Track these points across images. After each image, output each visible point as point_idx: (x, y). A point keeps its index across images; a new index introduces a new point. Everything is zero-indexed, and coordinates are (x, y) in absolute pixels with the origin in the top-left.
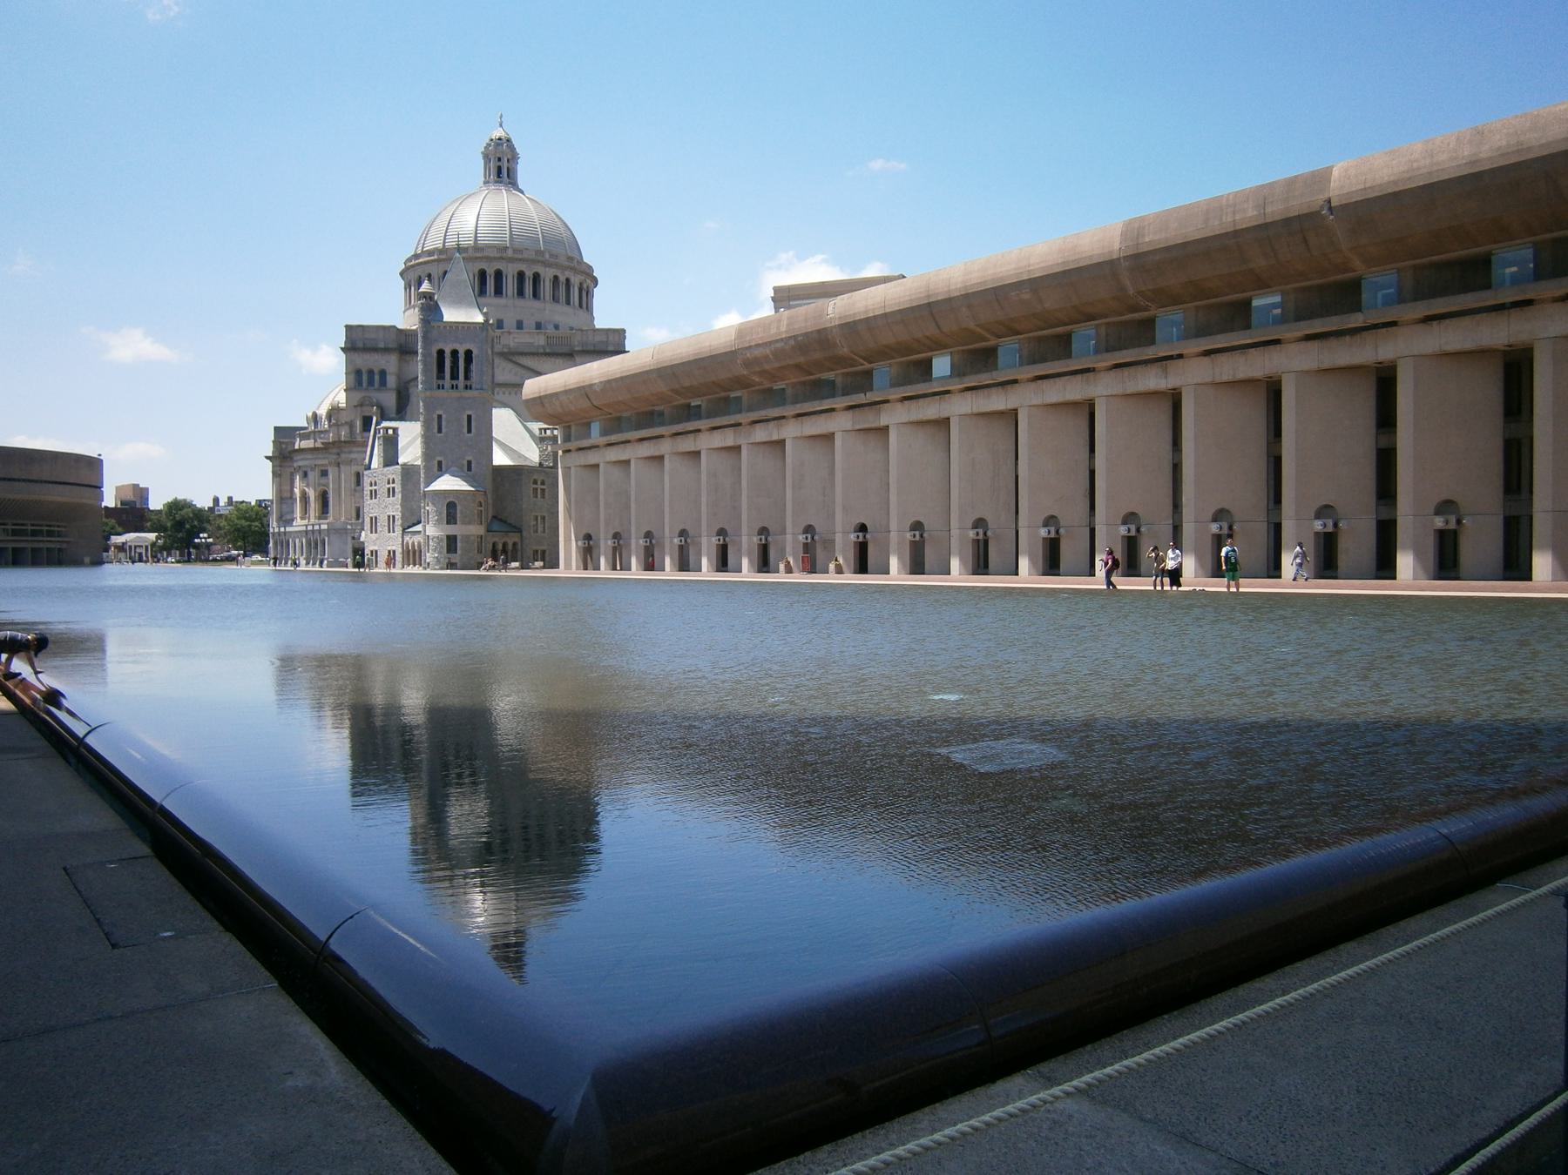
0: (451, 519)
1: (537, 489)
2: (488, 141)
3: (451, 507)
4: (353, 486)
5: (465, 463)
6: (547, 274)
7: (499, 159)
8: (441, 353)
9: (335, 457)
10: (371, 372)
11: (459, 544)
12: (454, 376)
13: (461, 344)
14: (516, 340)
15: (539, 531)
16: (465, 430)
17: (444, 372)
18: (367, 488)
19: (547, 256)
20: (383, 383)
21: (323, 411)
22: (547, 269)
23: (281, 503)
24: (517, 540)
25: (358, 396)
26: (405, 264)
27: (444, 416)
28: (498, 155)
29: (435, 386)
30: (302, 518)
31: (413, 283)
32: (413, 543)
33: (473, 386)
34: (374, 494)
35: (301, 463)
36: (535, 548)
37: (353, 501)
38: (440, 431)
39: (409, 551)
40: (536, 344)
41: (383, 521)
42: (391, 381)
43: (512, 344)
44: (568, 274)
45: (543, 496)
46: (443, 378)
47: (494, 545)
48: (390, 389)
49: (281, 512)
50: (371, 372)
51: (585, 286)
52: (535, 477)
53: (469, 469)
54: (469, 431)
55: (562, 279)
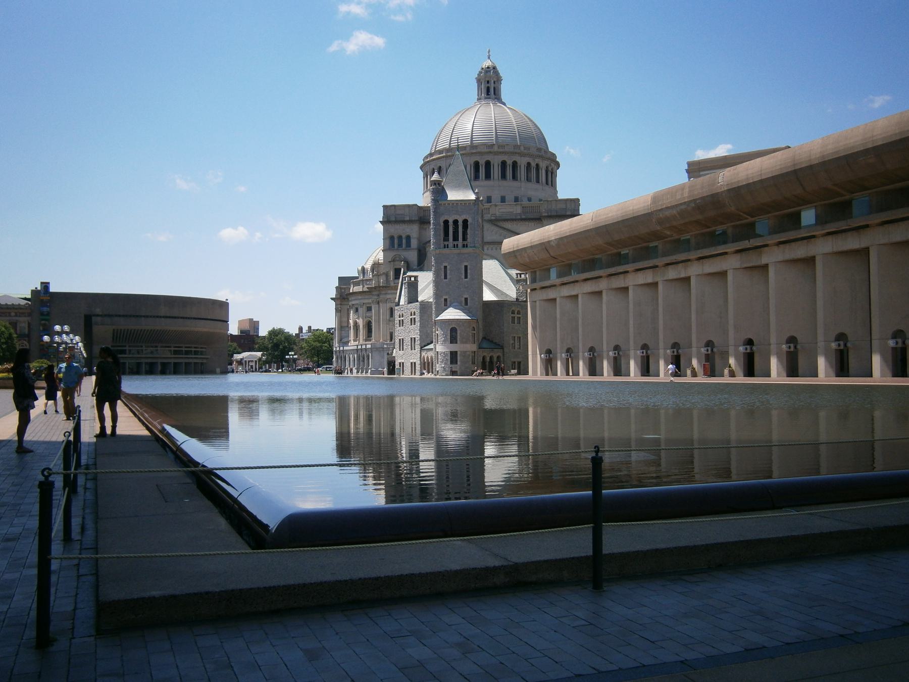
0: (453, 340)
1: (514, 317)
2: (480, 70)
3: (453, 331)
6: (522, 162)
7: (488, 82)
8: (446, 223)
9: (376, 297)
10: (400, 237)
12: (456, 238)
13: (460, 215)
14: (501, 210)
15: (516, 348)
16: (463, 277)
18: (397, 319)
19: (522, 148)
20: (408, 244)
21: (368, 266)
22: (522, 158)
23: (341, 330)
24: (501, 354)
25: (392, 254)
26: (423, 160)
27: (448, 267)
28: (487, 79)
29: (442, 246)
30: (354, 341)
31: (429, 173)
32: (428, 357)
33: (469, 246)
34: (401, 323)
35: (354, 302)
36: (513, 360)
38: (446, 277)
39: (425, 363)
40: (515, 213)
41: (407, 342)
42: (414, 243)
44: (537, 160)
45: (519, 323)
47: (484, 358)
49: (341, 336)
51: (550, 169)
52: (513, 308)
53: (466, 303)
54: (466, 277)
55: (533, 165)
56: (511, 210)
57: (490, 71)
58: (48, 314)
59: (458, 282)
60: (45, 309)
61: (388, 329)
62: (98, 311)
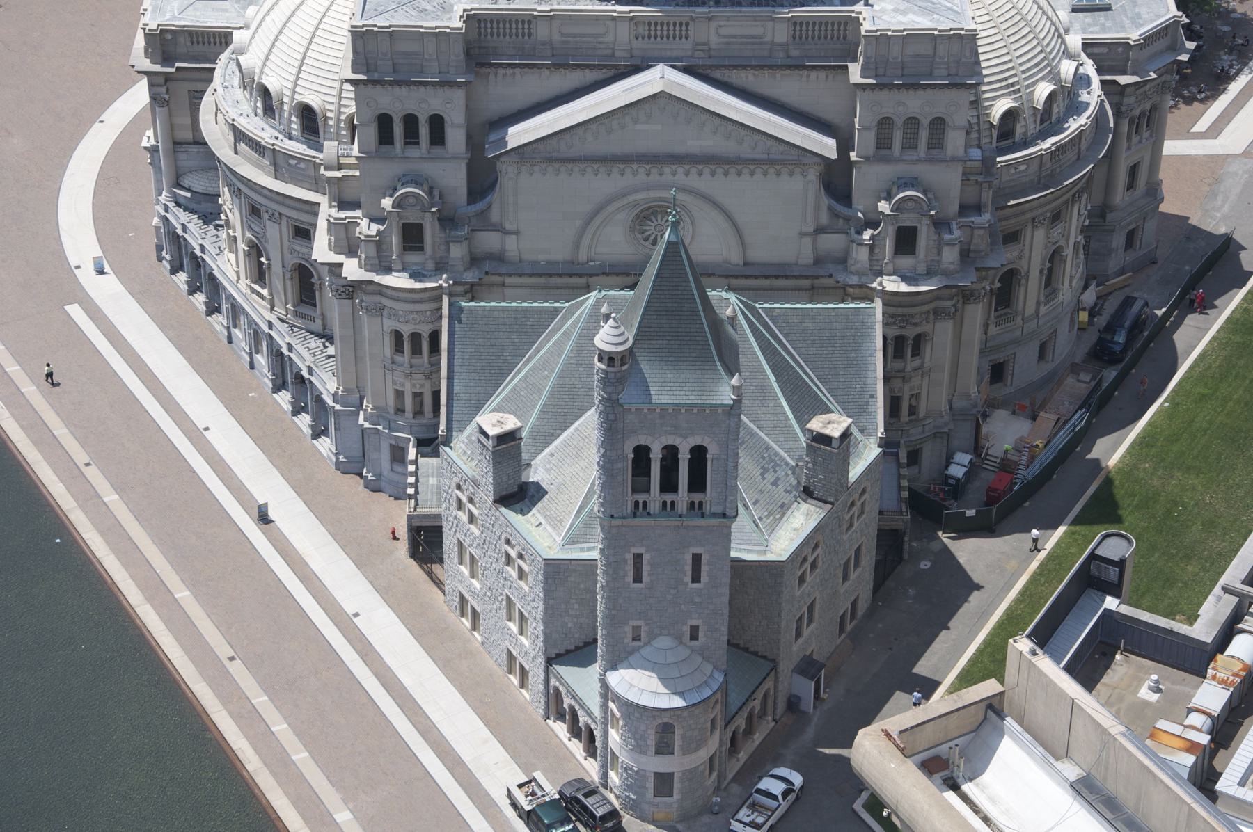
3: (666, 730)
5: (687, 629)
8: (642, 454)
10: (411, 122)
11: (677, 786)
12: (669, 484)
14: (723, 31)
16: (688, 578)
17: (648, 474)
27: (646, 557)
29: (630, 507)
33: (707, 508)
37: (389, 377)
38: (638, 578)
40: (768, 39)
42: (456, 138)
43: (714, 41)
46: (648, 490)
48: (455, 157)
49: (176, 167)
53: (694, 637)
54: (696, 578)
56: (758, 31)
59: (673, 592)
61: (389, 384)
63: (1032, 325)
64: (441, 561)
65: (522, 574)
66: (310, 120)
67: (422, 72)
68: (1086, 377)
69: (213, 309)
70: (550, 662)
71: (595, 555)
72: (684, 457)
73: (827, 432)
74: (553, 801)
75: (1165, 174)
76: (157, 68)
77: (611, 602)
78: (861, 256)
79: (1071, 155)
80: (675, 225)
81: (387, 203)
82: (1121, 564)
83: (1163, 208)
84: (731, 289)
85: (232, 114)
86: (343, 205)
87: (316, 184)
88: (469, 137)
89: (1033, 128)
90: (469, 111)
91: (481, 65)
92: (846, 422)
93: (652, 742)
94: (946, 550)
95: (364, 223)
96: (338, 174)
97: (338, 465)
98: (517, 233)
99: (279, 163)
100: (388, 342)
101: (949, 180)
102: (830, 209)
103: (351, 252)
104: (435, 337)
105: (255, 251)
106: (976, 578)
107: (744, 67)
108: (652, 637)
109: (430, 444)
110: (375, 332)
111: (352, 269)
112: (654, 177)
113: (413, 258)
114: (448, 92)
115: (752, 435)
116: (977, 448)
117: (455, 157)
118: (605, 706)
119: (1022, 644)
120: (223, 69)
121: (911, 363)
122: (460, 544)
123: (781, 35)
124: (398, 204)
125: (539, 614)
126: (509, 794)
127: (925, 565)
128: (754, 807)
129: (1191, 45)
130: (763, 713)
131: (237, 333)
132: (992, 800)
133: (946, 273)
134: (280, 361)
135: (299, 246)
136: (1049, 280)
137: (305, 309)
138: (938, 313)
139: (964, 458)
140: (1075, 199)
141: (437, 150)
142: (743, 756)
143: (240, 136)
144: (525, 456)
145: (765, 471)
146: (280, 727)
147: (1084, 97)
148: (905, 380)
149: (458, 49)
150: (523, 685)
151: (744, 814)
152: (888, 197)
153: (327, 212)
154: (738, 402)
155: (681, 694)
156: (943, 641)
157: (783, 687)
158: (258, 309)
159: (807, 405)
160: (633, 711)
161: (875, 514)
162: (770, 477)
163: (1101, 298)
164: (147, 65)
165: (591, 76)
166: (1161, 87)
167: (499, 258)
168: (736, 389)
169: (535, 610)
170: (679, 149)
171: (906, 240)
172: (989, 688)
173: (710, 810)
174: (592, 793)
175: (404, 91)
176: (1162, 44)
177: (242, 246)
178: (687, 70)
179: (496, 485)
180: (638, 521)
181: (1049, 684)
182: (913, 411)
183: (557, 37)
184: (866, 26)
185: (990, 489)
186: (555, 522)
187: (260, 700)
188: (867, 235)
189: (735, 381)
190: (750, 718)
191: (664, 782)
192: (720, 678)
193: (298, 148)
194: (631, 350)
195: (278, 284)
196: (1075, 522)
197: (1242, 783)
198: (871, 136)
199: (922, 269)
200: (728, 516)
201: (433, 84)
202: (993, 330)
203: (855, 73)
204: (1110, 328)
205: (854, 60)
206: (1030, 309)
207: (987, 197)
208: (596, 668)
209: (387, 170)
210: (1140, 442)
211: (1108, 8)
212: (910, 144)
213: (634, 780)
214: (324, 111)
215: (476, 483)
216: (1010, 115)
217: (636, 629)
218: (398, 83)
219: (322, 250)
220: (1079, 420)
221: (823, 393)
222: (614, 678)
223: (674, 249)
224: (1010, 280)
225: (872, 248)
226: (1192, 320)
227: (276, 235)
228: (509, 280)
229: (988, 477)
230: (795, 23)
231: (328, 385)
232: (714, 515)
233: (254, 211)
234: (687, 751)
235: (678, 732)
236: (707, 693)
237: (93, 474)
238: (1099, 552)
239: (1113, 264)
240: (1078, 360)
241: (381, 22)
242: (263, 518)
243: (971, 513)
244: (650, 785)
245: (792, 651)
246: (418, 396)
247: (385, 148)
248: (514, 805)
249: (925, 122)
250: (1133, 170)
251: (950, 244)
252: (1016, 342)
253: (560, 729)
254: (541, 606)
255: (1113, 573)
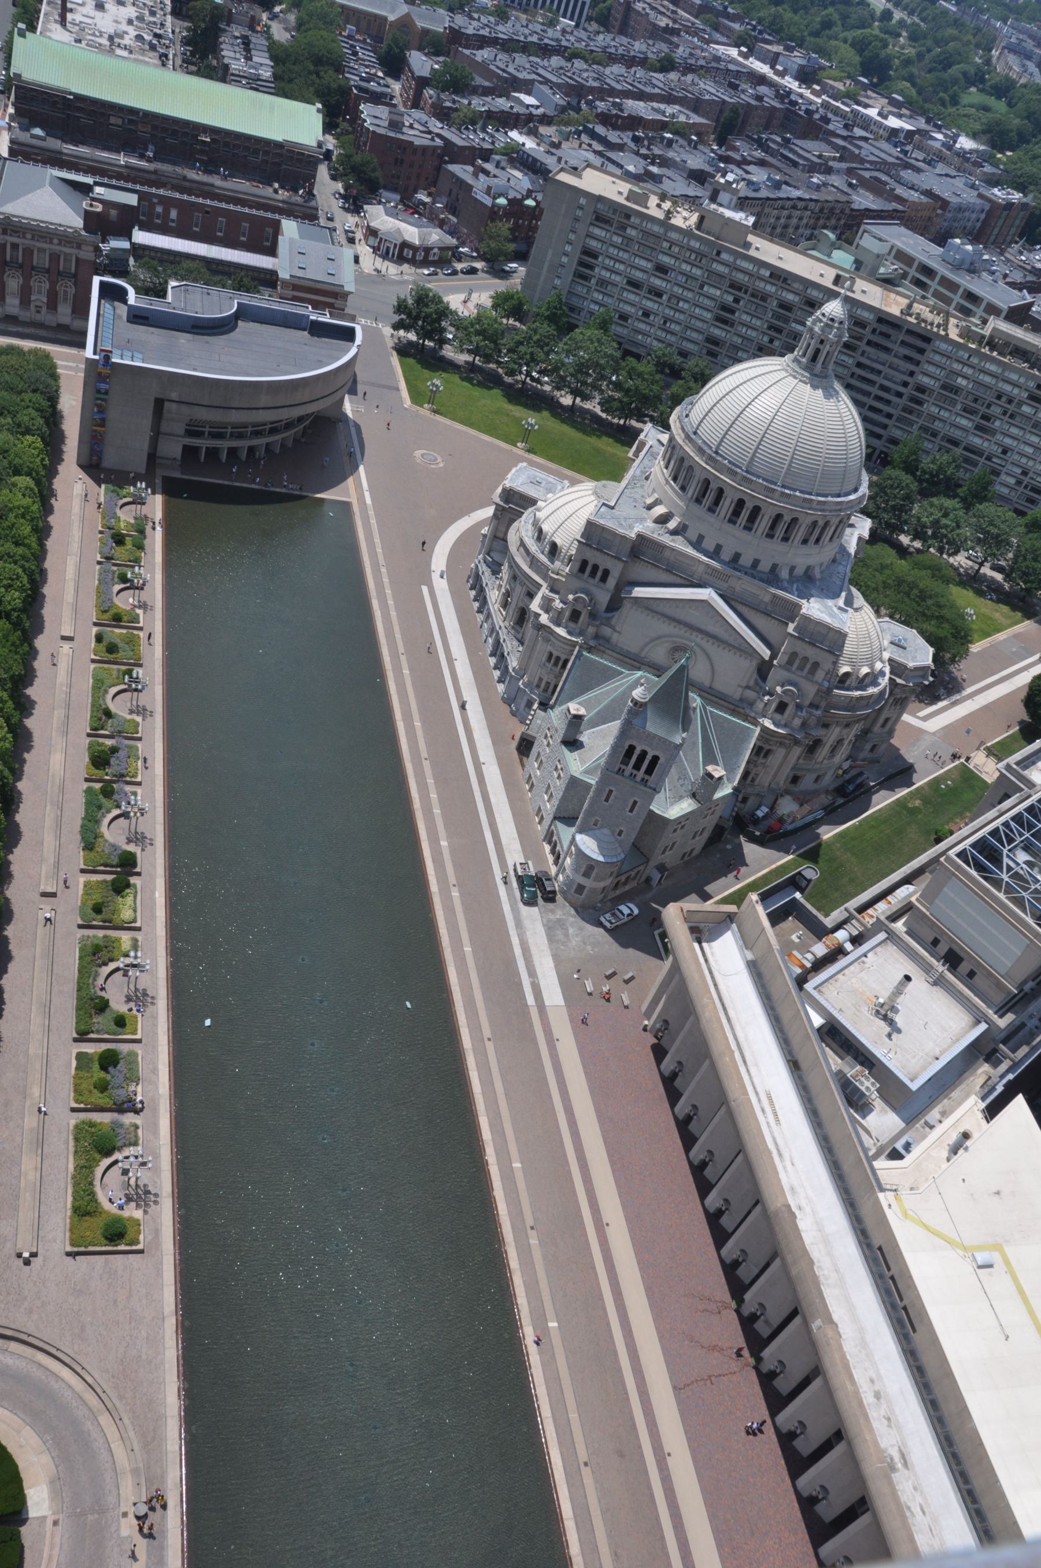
4: (544, 659)
5: (618, 830)
8: (632, 748)
10: (595, 568)
11: (585, 892)
12: (637, 766)
16: (628, 809)
27: (614, 793)
29: (616, 769)
33: (649, 784)
38: (607, 800)
42: (611, 582)
43: (738, 589)
48: (607, 590)
50: (595, 568)
53: (620, 834)
54: (631, 811)
57: (831, 327)
58: (106, 393)
60: (103, 386)
62: (174, 396)
63: (818, 766)
64: (528, 757)
65: (559, 777)
66: (554, 550)
67: (609, 549)
68: (830, 797)
69: (479, 611)
70: (555, 818)
71: (593, 782)
72: (649, 758)
73: (713, 773)
74: (531, 876)
75: (898, 727)
76: (501, 503)
77: (591, 805)
78: (760, 706)
79: (864, 702)
80: (688, 658)
81: (571, 597)
82: (809, 881)
83: (892, 741)
84: (699, 696)
85: (524, 534)
86: (552, 590)
87: (545, 577)
88: (617, 584)
89: (854, 684)
90: (622, 574)
91: (635, 556)
92: (723, 773)
93: (583, 870)
94: (740, 845)
95: (558, 601)
96: (556, 577)
97: (503, 698)
98: (620, 633)
99: (534, 562)
100: (546, 655)
101: (811, 690)
102: (756, 680)
103: (547, 611)
104: (566, 662)
105: (508, 594)
106: (748, 862)
107: (745, 605)
108: (602, 827)
109: (544, 706)
110: (542, 649)
111: (544, 619)
112: (688, 634)
113: (572, 625)
114: (616, 562)
115: (682, 761)
116: (772, 808)
117: (607, 590)
118: (569, 848)
119: (754, 897)
120: (528, 515)
121: (761, 760)
122: (539, 754)
123: (767, 599)
124: (575, 600)
125: (559, 796)
126: (515, 865)
127: (729, 847)
128: (614, 915)
129: (931, 679)
130: (634, 878)
131: (485, 625)
132: (712, 954)
133: (792, 729)
134: (497, 644)
135: (526, 599)
136: (833, 750)
137: (517, 627)
138: (781, 744)
139: (765, 809)
140: (858, 721)
141: (602, 584)
142: (618, 892)
143: (522, 544)
144: (582, 728)
145: (680, 778)
146: (434, 796)
147: (880, 680)
148: (755, 766)
149: (628, 546)
150: (540, 823)
151: (608, 916)
152: (782, 686)
153: (544, 591)
154: (681, 745)
155: (604, 856)
156: (722, 881)
157: (647, 872)
158: (500, 618)
159: (710, 758)
160: (580, 853)
161: (718, 817)
162: (681, 782)
163: (851, 767)
164: (498, 500)
165: (679, 581)
166: (912, 691)
167: (608, 640)
168: (683, 739)
169: (558, 795)
170: (703, 627)
171: (781, 707)
172: (732, 908)
173: (594, 908)
174: (549, 879)
175: (598, 554)
176: (921, 673)
177: (503, 590)
178: (721, 596)
179: (565, 735)
180: (617, 776)
181: (758, 917)
182: (753, 780)
183: (672, 558)
184: (804, 611)
185: (770, 827)
186: (583, 762)
187: (430, 781)
188: (767, 698)
189: (684, 735)
190: (628, 878)
191: (580, 889)
192: (623, 856)
193: (544, 559)
194: (646, 703)
195: (511, 613)
196: (799, 856)
197: (815, 988)
198: (786, 658)
199: (783, 722)
200: (656, 790)
201: (612, 556)
202: (801, 761)
203: (791, 628)
204: (849, 781)
205: (793, 622)
206: (820, 759)
207: (823, 704)
208: (573, 829)
209: (577, 584)
210: (840, 835)
211: (905, 648)
212: (801, 668)
213: (569, 882)
214: (561, 548)
215: (556, 730)
216: (847, 675)
217: (597, 821)
218: (597, 549)
219: (535, 606)
220: (820, 814)
221: (719, 756)
222: (580, 838)
223: (683, 668)
224: (817, 743)
225: (766, 704)
226: (883, 793)
227: (519, 591)
228: (607, 651)
229: (771, 822)
230: (775, 596)
231: (513, 663)
232: (650, 788)
233: (514, 578)
234: (595, 880)
235: (595, 871)
236: (615, 860)
237: (403, 659)
238: (803, 873)
239: (862, 755)
240: (831, 788)
241: (602, 522)
242: (463, 706)
243: (758, 833)
244: (574, 887)
245: (657, 858)
246: (548, 683)
247: (580, 574)
248: (515, 870)
249: (811, 662)
250: (887, 720)
251: (799, 717)
252: (808, 770)
253: (547, 848)
254: (561, 794)
255: (804, 883)
